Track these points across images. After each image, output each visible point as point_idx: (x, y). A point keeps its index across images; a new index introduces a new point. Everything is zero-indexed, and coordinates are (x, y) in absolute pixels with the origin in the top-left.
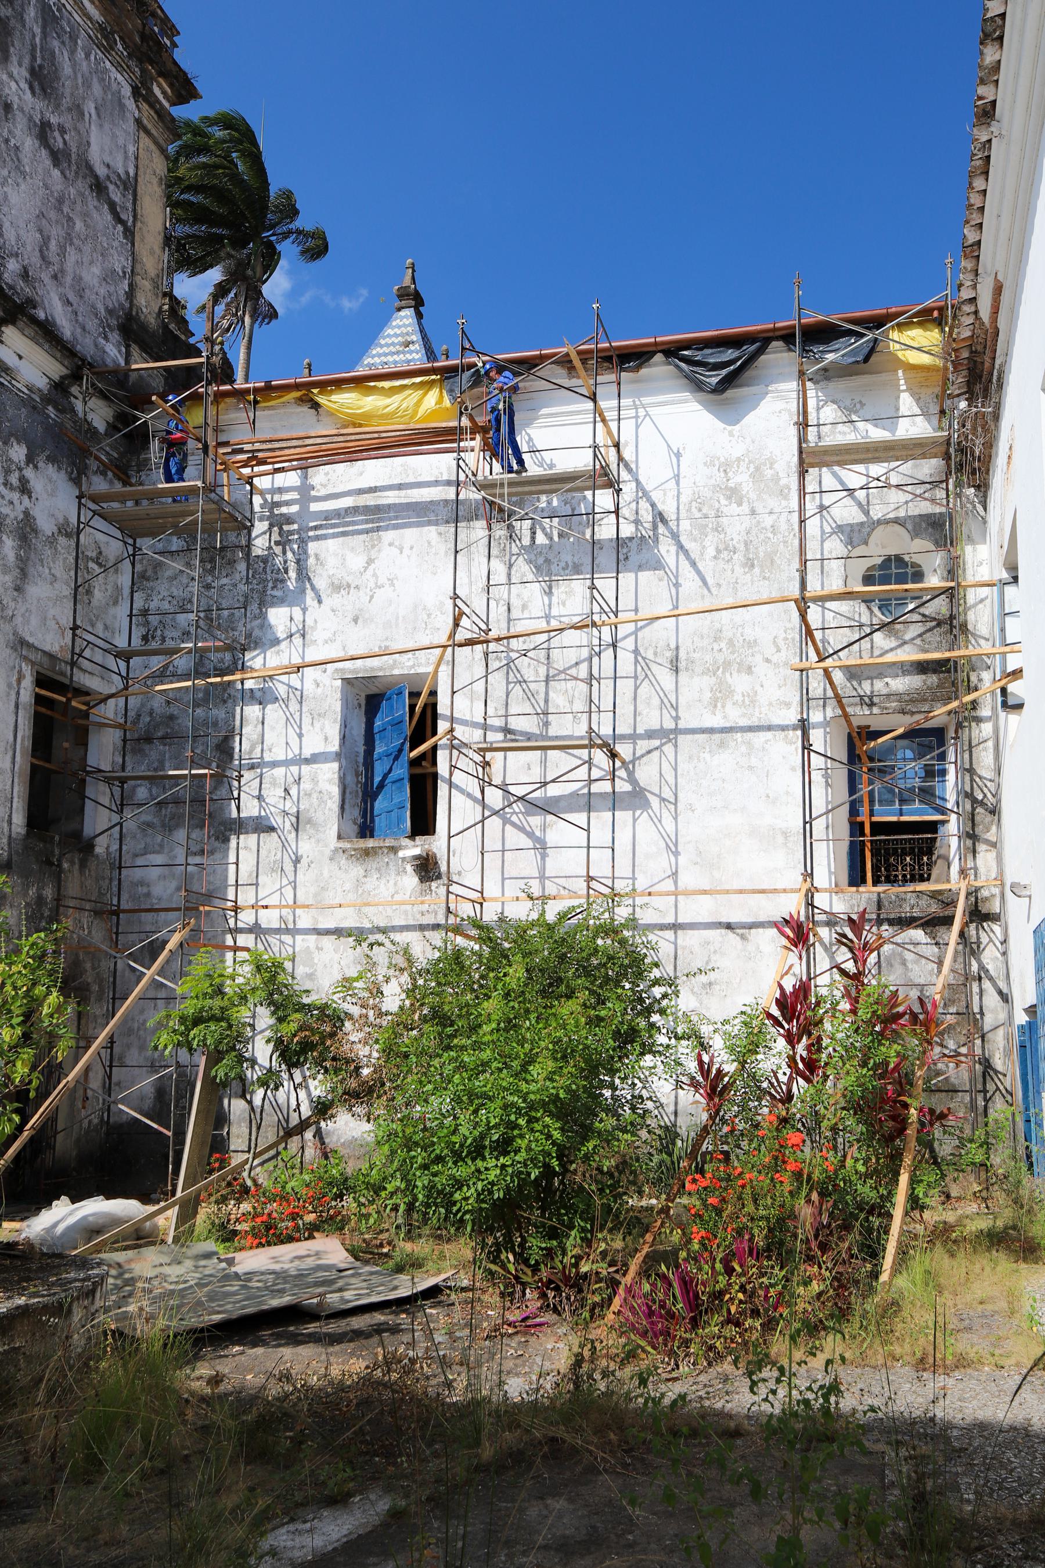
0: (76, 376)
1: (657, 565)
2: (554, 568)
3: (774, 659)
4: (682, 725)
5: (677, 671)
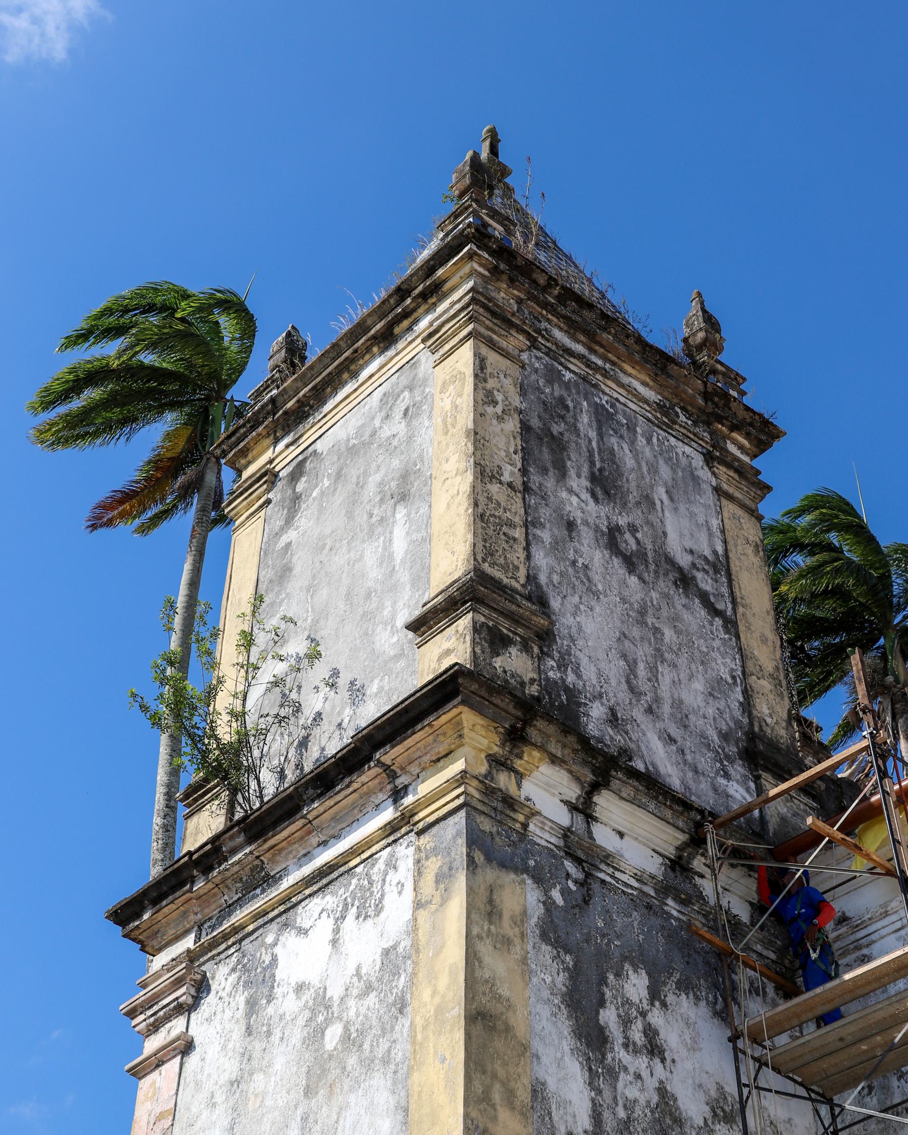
0: (697, 841)
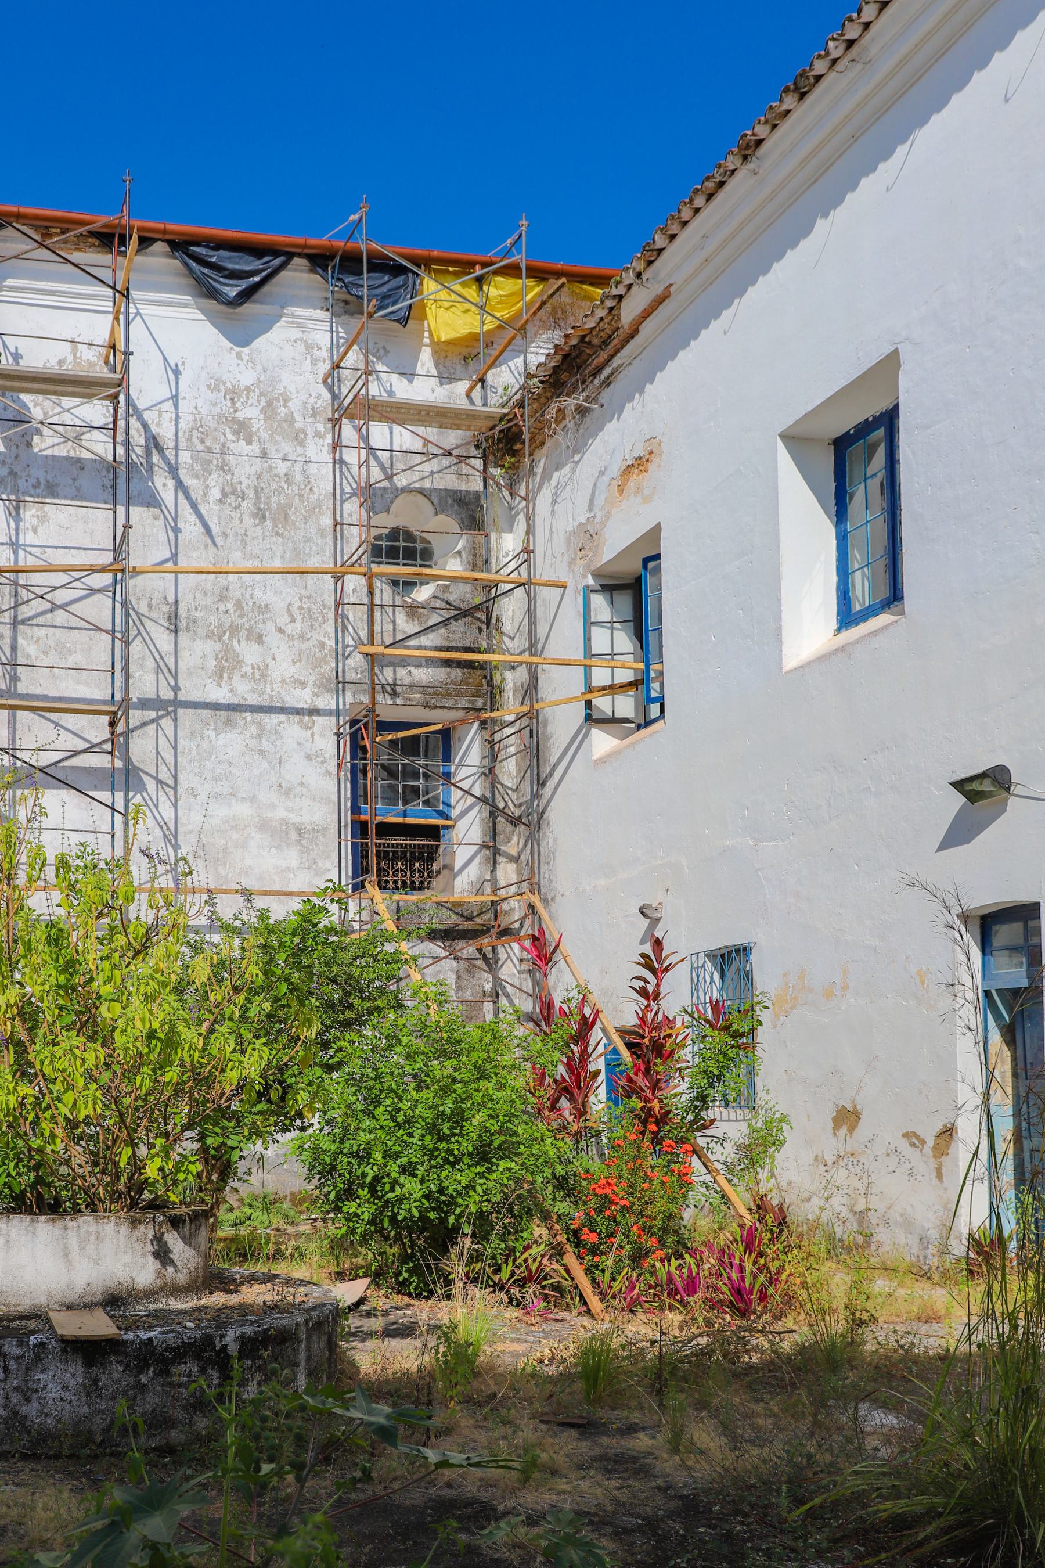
1: (152, 501)
2: (21, 483)
3: (288, 629)
4: (181, 697)
5: (176, 631)
